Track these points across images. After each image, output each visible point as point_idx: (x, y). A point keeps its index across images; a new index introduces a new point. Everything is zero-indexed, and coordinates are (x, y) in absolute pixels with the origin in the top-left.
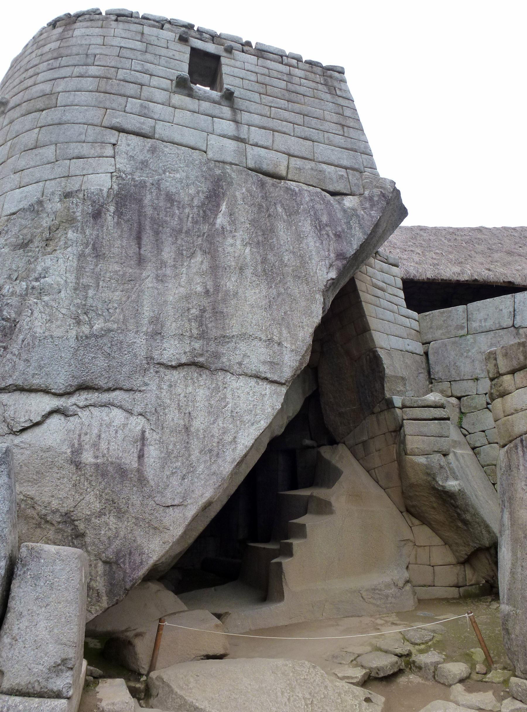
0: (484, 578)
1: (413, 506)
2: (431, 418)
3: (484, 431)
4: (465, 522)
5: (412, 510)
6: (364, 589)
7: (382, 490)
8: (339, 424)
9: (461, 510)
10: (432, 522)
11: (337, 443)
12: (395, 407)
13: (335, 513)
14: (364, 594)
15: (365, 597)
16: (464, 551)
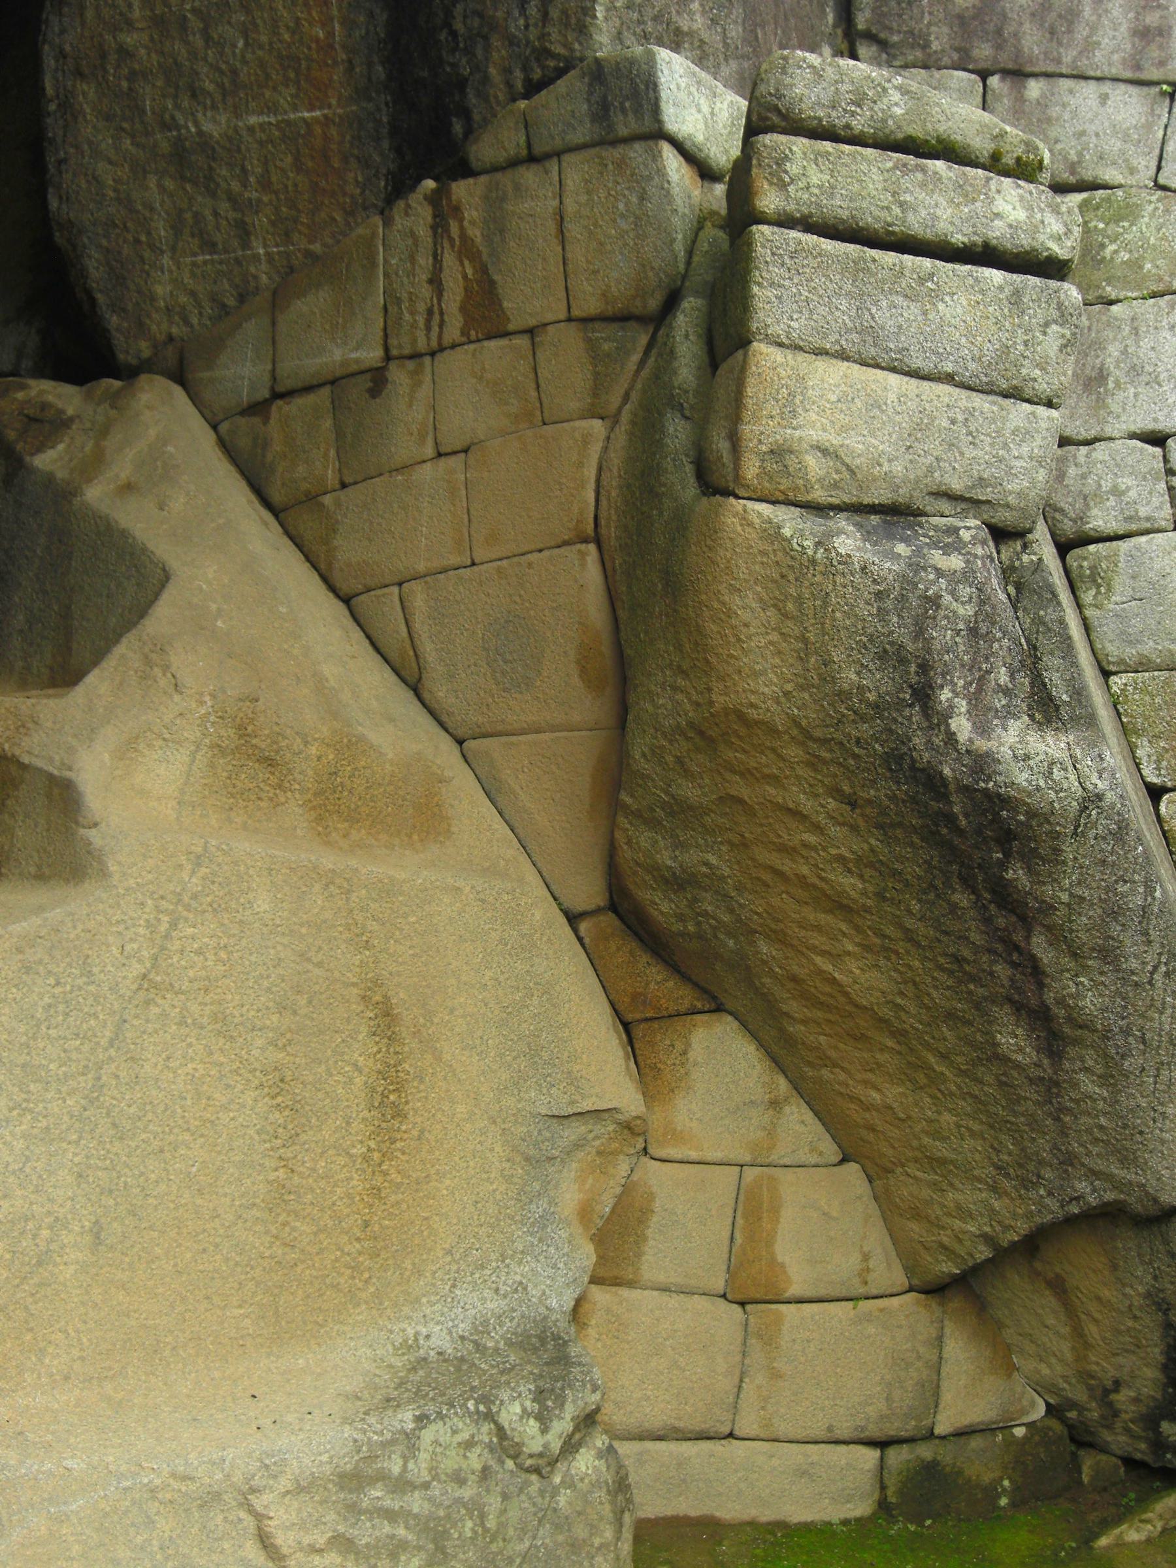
0: (1041, 1387)
1: (678, 882)
2: (958, 239)
3: (1157, 439)
4: (1052, 1030)
5: (663, 907)
6: (285, 1483)
7: (446, 744)
8: (162, 230)
9: (1059, 937)
10: (793, 1007)
11: (129, 373)
12: (660, 134)
13: (104, 874)
14: (283, 1518)
15: (284, 1540)
16: (978, 1214)
